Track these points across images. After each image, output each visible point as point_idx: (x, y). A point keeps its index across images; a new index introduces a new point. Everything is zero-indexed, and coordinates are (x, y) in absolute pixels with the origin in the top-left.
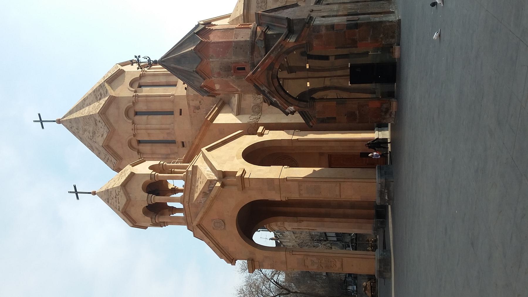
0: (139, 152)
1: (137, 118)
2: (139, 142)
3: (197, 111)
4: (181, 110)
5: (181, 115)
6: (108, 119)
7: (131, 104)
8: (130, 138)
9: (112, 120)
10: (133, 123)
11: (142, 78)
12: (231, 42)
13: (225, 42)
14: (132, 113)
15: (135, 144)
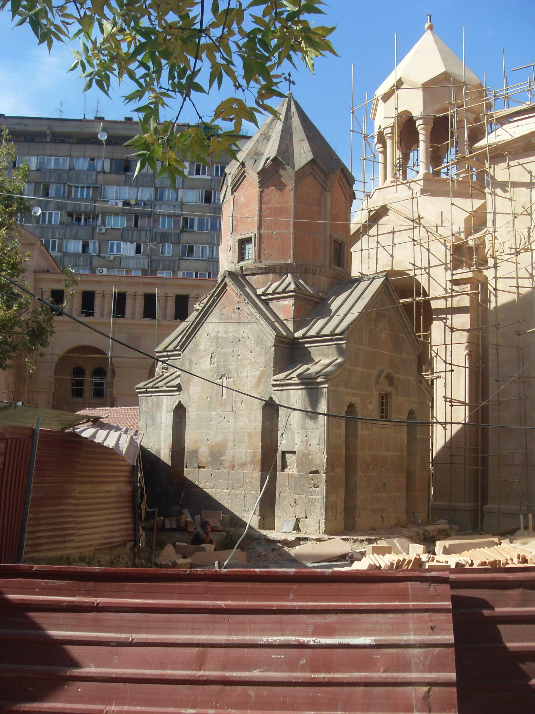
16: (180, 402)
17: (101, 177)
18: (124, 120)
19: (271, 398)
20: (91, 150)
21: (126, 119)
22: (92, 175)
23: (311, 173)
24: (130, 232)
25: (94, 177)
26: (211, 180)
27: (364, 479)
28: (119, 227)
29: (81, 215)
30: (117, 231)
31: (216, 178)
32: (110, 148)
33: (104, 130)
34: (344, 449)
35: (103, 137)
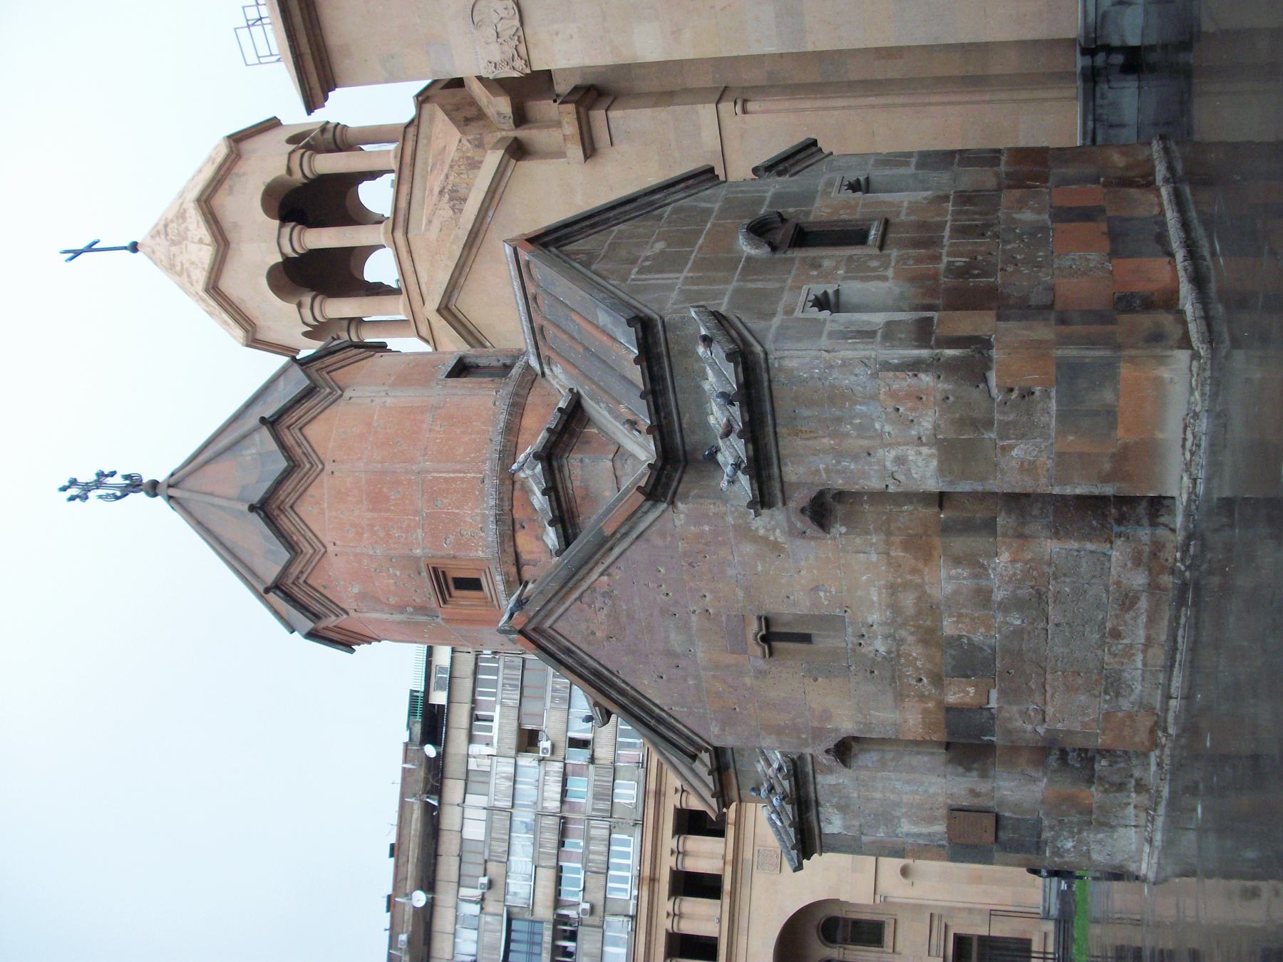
16: (827, 751)
17: (491, 906)
18: (392, 860)
19: (803, 510)
20: (444, 920)
21: (392, 855)
22: (486, 923)
23: (300, 429)
24: (591, 857)
25: (489, 919)
26: (502, 704)
27: (1010, 269)
28: (582, 876)
29: (558, 947)
30: (588, 880)
31: (499, 696)
32: (441, 886)
33: (408, 895)
34: (929, 314)
35: (420, 899)
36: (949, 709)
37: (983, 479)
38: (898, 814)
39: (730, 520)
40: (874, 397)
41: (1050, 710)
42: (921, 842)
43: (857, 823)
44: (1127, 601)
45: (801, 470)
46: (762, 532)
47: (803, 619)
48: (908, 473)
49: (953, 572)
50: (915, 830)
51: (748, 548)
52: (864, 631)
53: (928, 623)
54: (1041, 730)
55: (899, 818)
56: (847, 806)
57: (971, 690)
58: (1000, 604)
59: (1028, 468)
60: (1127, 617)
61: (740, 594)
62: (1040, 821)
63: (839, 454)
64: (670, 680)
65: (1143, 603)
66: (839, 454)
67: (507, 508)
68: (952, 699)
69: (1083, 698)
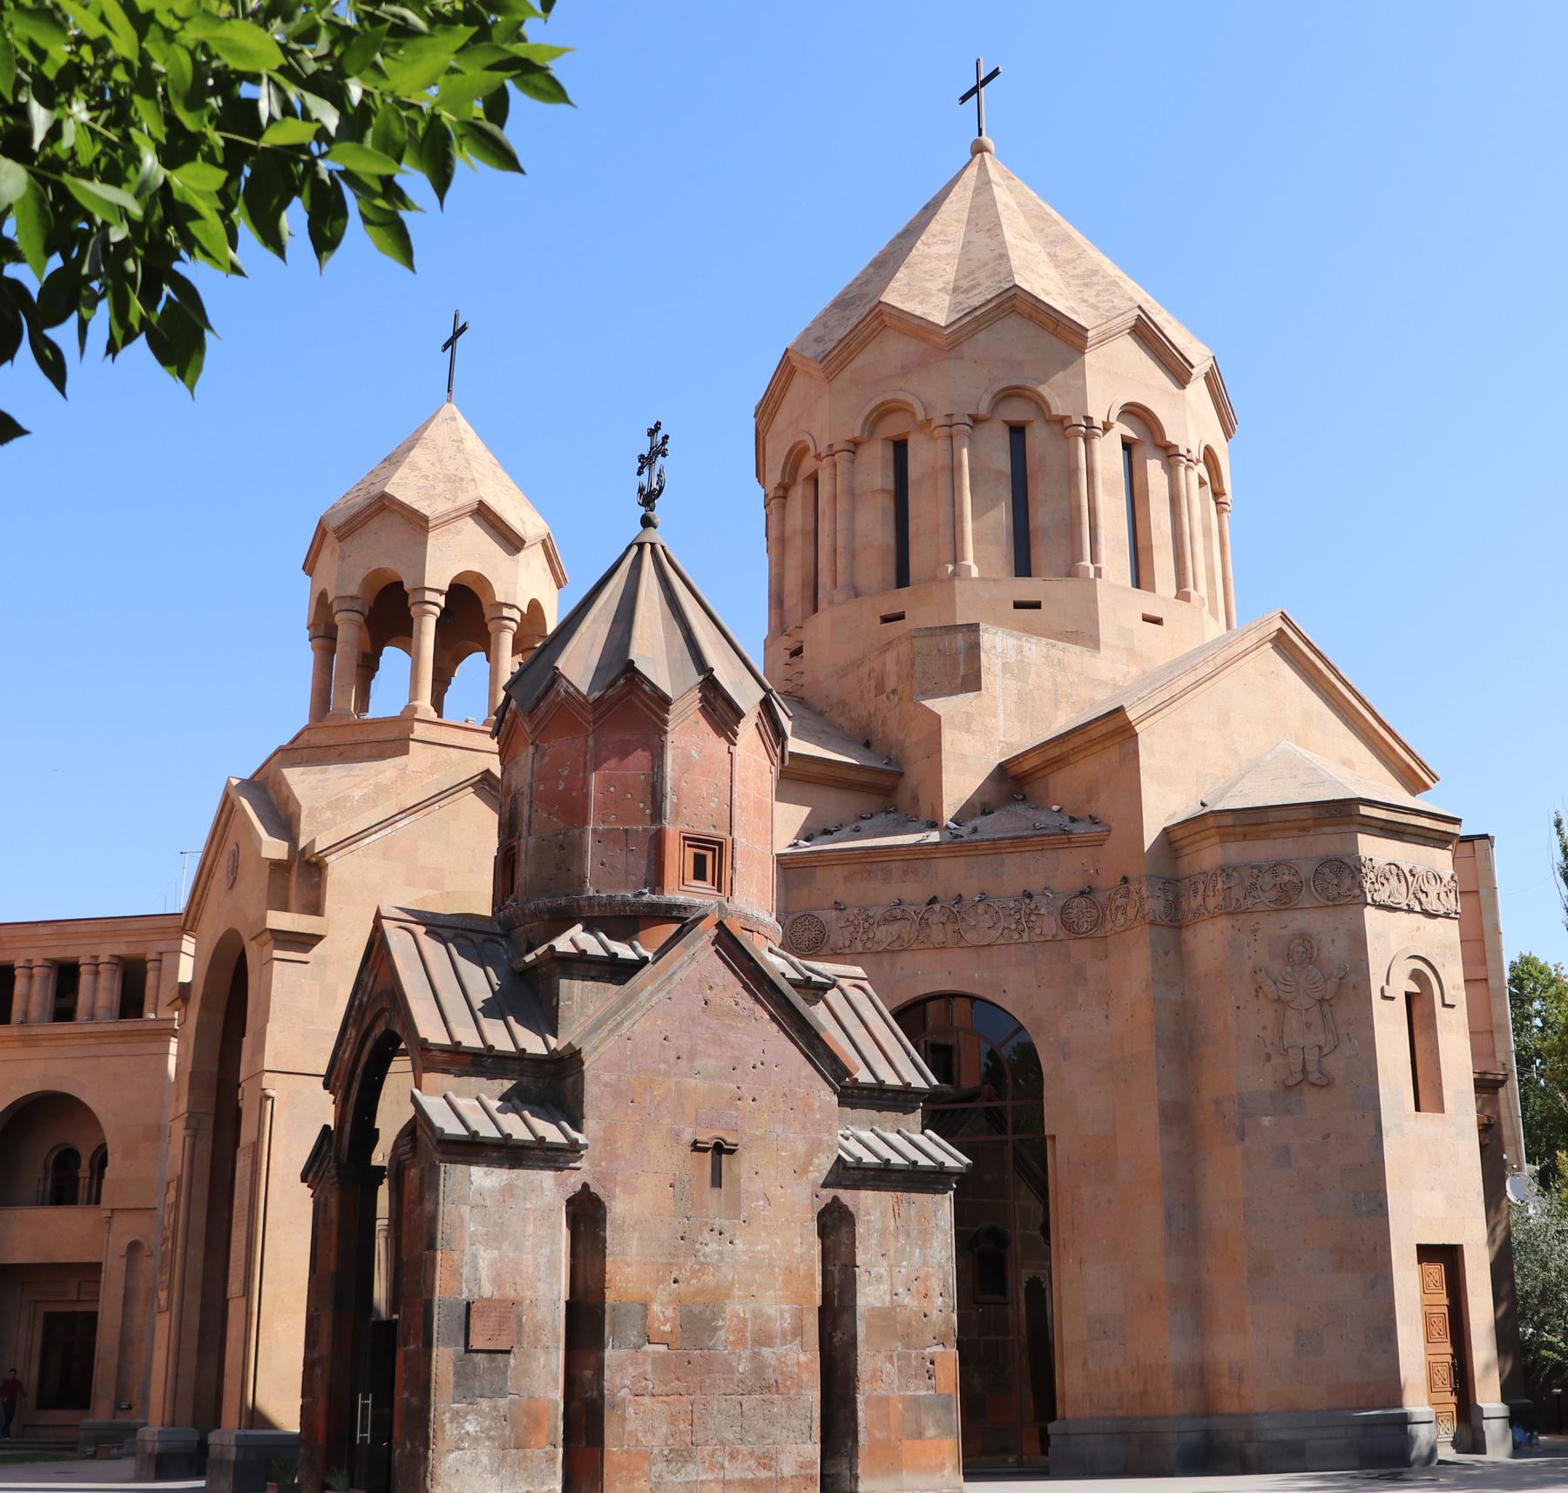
0: (784, 490)
1: (877, 457)
2: (814, 479)
3: (873, 684)
4: (901, 617)
5: (886, 619)
6: (864, 344)
7: (920, 416)
8: (812, 446)
9: (862, 360)
10: (855, 446)
11: (1057, 427)
12: (585, 822)
13: (586, 795)
14: (894, 426)
15: (808, 464)
16: (585, 1186)
19: (835, 1199)
36: (645, 1306)
37: (867, 1341)
38: (505, 1247)
39: (826, 1137)
40: (925, 1264)
41: (647, 1400)
42: (465, 1270)
43: (488, 1202)
44: (766, 1461)
45: (869, 1202)
46: (816, 1161)
47: (736, 1181)
48: (869, 1283)
49: (787, 1315)
50: (483, 1264)
51: (801, 1148)
52: (726, 1235)
53: (737, 1292)
54: (624, 1393)
55: (499, 1248)
56: (512, 1195)
57: (667, 1328)
58: (759, 1354)
59: (877, 1376)
60: (752, 1462)
61: (758, 1133)
62: (502, 1393)
63: (883, 1232)
64: (662, 1046)
65: (764, 1474)
66: (883, 1232)
67: (761, 929)
68: (656, 1308)
69: (663, 1429)
